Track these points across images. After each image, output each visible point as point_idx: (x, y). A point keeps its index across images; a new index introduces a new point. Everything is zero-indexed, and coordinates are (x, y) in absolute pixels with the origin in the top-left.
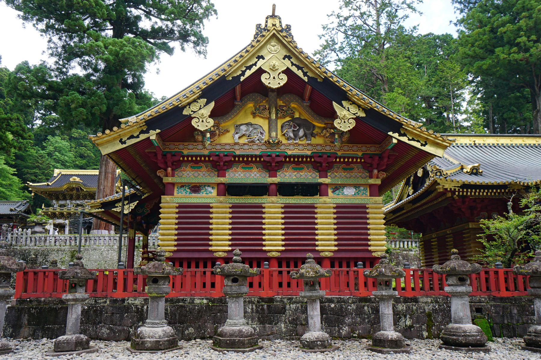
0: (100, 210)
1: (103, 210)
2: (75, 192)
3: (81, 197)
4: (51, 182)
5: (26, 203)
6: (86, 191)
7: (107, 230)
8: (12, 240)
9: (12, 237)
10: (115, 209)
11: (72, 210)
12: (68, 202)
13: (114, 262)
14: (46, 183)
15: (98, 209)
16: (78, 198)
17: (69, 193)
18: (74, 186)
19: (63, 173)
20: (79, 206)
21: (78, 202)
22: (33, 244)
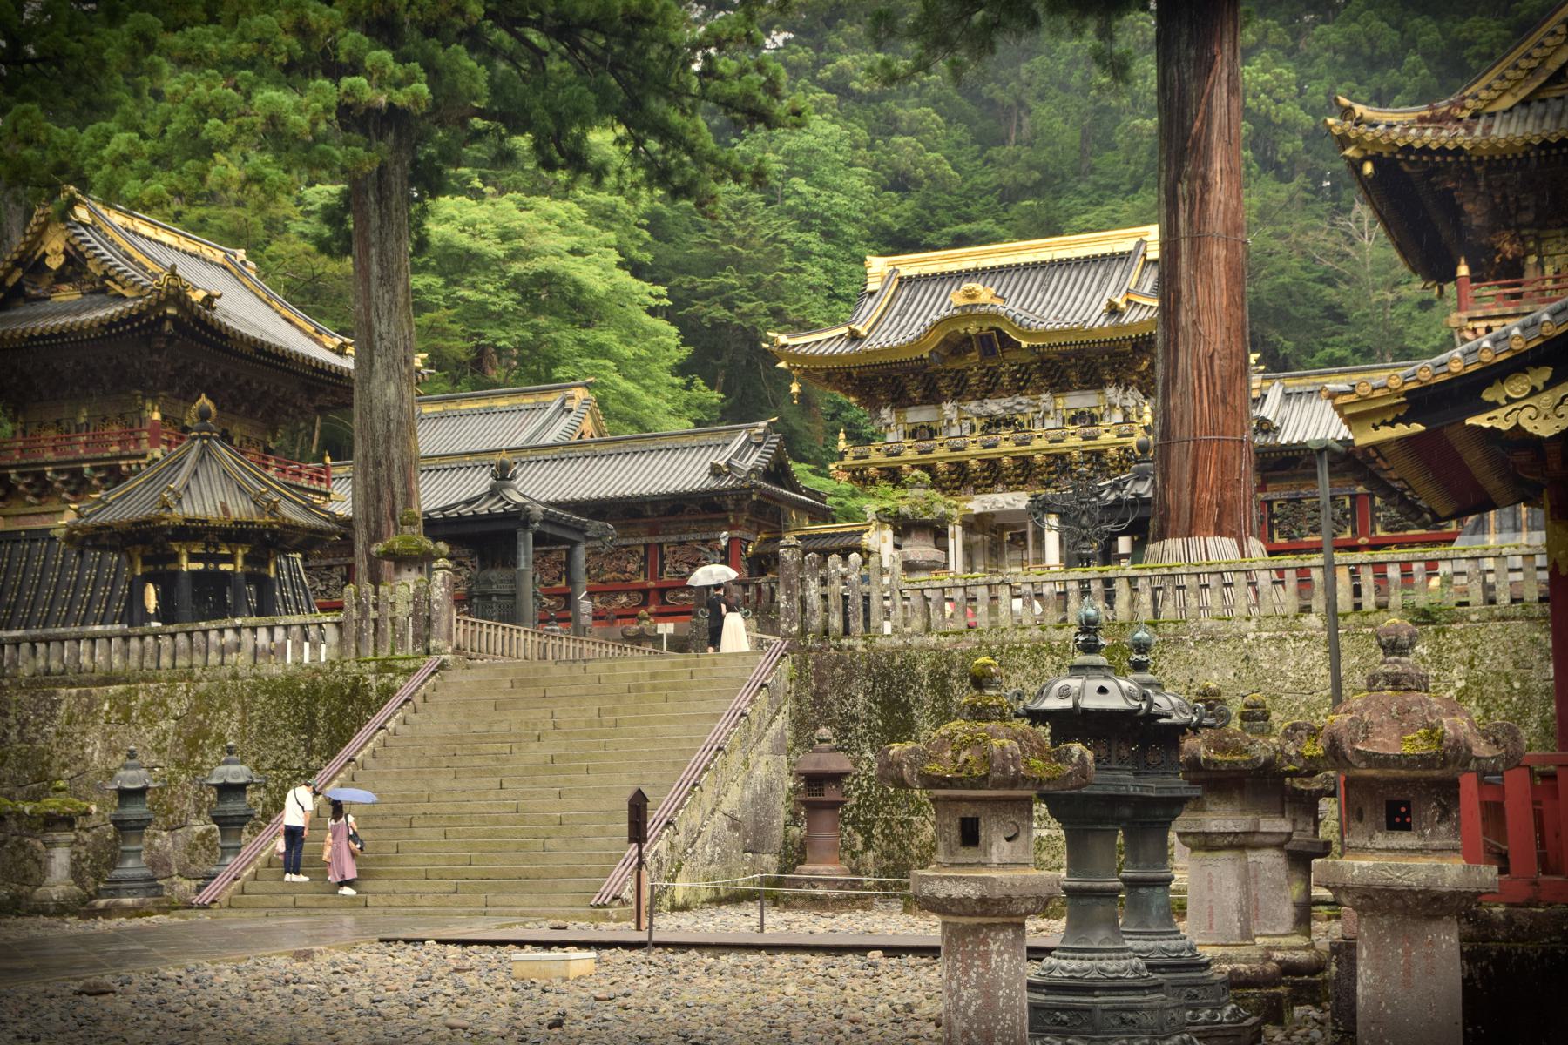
0: (1401, 430)
1: (1418, 428)
2: (974, 357)
3: (1005, 378)
5: (765, 435)
6: (1032, 348)
7: (1231, 535)
8: (826, 610)
9: (825, 597)
10: (1482, 421)
11: (973, 449)
12: (948, 408)
13: (1316, 697)
14: (845, 330)
15: (1392, 424)
16: (990, 389)
17: (949, 366)
18: (973, 329)
19: (905, 272)
20: (998, 425)
21: (994, 407)
22: (917, 623)
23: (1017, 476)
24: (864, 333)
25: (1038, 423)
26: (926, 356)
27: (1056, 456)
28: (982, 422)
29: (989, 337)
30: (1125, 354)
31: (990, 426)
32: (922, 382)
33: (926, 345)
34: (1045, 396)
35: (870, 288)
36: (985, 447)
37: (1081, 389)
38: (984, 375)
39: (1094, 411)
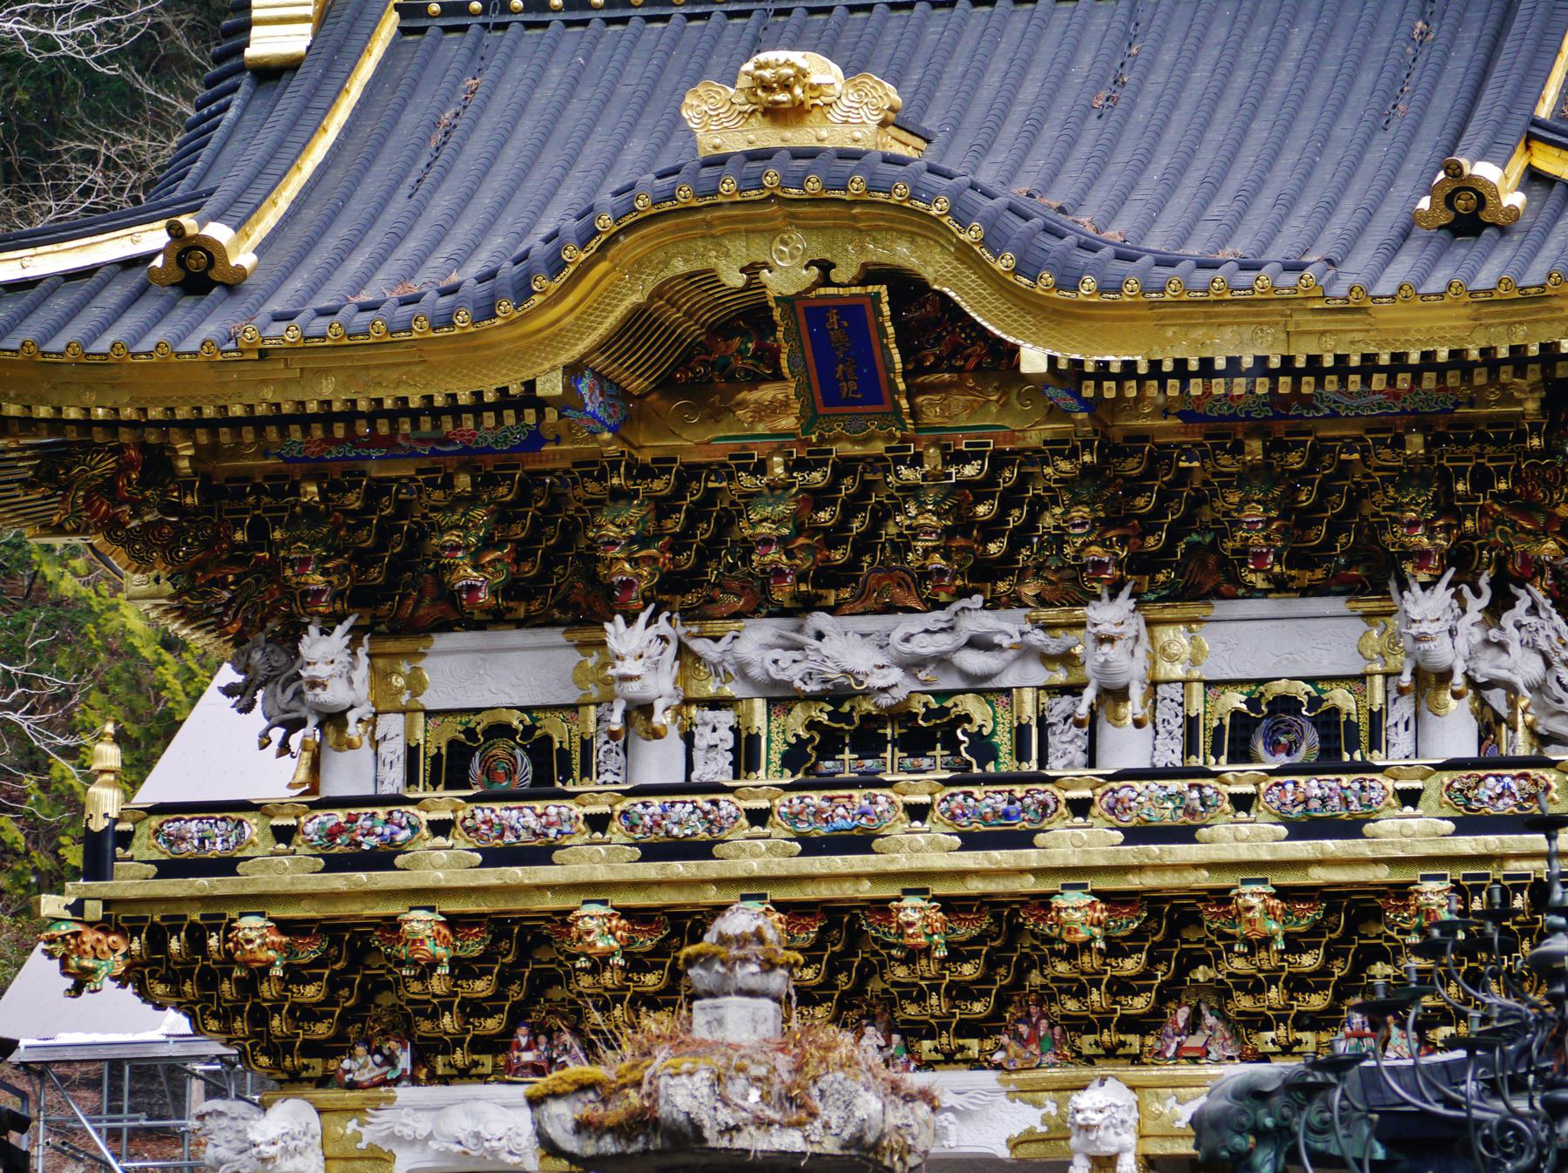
3: (923, 517)
4: (239, 214)
6: (1068, 376)
17: (650, 448)
20: (868, 740)
23: (961, 992)
24: (243, 258)
25: (1066, 751)
26: (551, 385)
27: (1152, 901)
28: (796, 722)
29: (856, 314)
30: (1509, 430)
31: (830, 744)
32: (504, 515)
33: (554, 338)
34: (1110, 614)
35: (264, 44)
36: (811, 846)
37: (1280, 586)
38: (819, 498)
39: (1341, 698)
